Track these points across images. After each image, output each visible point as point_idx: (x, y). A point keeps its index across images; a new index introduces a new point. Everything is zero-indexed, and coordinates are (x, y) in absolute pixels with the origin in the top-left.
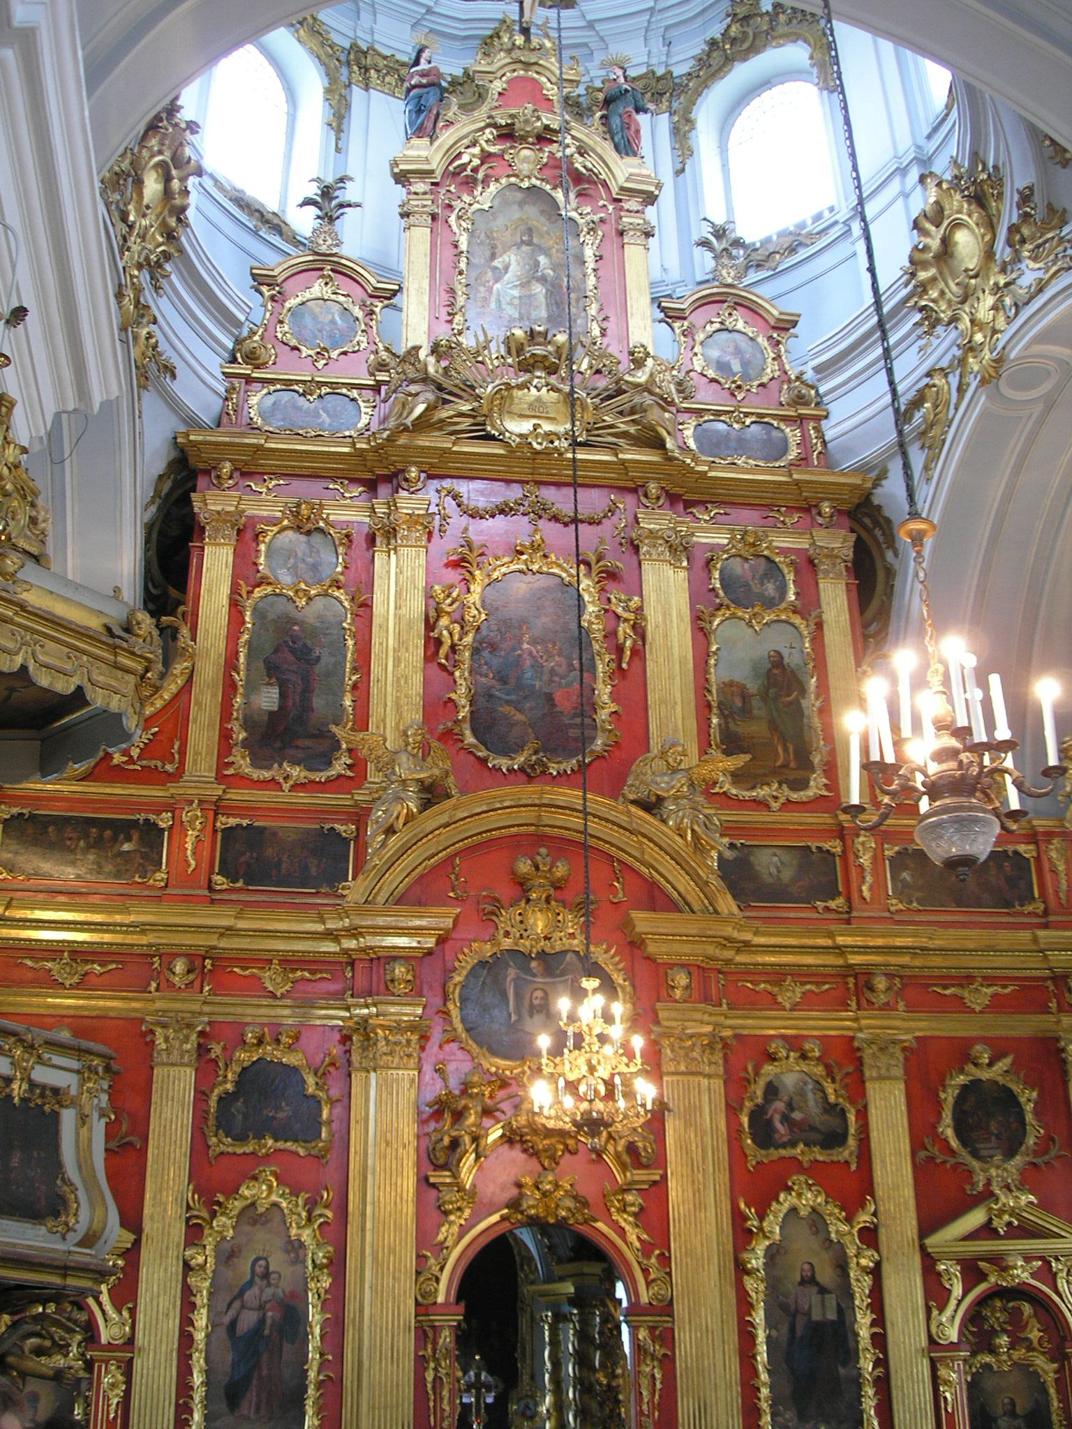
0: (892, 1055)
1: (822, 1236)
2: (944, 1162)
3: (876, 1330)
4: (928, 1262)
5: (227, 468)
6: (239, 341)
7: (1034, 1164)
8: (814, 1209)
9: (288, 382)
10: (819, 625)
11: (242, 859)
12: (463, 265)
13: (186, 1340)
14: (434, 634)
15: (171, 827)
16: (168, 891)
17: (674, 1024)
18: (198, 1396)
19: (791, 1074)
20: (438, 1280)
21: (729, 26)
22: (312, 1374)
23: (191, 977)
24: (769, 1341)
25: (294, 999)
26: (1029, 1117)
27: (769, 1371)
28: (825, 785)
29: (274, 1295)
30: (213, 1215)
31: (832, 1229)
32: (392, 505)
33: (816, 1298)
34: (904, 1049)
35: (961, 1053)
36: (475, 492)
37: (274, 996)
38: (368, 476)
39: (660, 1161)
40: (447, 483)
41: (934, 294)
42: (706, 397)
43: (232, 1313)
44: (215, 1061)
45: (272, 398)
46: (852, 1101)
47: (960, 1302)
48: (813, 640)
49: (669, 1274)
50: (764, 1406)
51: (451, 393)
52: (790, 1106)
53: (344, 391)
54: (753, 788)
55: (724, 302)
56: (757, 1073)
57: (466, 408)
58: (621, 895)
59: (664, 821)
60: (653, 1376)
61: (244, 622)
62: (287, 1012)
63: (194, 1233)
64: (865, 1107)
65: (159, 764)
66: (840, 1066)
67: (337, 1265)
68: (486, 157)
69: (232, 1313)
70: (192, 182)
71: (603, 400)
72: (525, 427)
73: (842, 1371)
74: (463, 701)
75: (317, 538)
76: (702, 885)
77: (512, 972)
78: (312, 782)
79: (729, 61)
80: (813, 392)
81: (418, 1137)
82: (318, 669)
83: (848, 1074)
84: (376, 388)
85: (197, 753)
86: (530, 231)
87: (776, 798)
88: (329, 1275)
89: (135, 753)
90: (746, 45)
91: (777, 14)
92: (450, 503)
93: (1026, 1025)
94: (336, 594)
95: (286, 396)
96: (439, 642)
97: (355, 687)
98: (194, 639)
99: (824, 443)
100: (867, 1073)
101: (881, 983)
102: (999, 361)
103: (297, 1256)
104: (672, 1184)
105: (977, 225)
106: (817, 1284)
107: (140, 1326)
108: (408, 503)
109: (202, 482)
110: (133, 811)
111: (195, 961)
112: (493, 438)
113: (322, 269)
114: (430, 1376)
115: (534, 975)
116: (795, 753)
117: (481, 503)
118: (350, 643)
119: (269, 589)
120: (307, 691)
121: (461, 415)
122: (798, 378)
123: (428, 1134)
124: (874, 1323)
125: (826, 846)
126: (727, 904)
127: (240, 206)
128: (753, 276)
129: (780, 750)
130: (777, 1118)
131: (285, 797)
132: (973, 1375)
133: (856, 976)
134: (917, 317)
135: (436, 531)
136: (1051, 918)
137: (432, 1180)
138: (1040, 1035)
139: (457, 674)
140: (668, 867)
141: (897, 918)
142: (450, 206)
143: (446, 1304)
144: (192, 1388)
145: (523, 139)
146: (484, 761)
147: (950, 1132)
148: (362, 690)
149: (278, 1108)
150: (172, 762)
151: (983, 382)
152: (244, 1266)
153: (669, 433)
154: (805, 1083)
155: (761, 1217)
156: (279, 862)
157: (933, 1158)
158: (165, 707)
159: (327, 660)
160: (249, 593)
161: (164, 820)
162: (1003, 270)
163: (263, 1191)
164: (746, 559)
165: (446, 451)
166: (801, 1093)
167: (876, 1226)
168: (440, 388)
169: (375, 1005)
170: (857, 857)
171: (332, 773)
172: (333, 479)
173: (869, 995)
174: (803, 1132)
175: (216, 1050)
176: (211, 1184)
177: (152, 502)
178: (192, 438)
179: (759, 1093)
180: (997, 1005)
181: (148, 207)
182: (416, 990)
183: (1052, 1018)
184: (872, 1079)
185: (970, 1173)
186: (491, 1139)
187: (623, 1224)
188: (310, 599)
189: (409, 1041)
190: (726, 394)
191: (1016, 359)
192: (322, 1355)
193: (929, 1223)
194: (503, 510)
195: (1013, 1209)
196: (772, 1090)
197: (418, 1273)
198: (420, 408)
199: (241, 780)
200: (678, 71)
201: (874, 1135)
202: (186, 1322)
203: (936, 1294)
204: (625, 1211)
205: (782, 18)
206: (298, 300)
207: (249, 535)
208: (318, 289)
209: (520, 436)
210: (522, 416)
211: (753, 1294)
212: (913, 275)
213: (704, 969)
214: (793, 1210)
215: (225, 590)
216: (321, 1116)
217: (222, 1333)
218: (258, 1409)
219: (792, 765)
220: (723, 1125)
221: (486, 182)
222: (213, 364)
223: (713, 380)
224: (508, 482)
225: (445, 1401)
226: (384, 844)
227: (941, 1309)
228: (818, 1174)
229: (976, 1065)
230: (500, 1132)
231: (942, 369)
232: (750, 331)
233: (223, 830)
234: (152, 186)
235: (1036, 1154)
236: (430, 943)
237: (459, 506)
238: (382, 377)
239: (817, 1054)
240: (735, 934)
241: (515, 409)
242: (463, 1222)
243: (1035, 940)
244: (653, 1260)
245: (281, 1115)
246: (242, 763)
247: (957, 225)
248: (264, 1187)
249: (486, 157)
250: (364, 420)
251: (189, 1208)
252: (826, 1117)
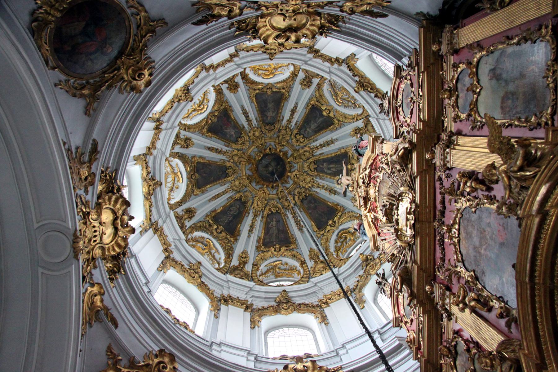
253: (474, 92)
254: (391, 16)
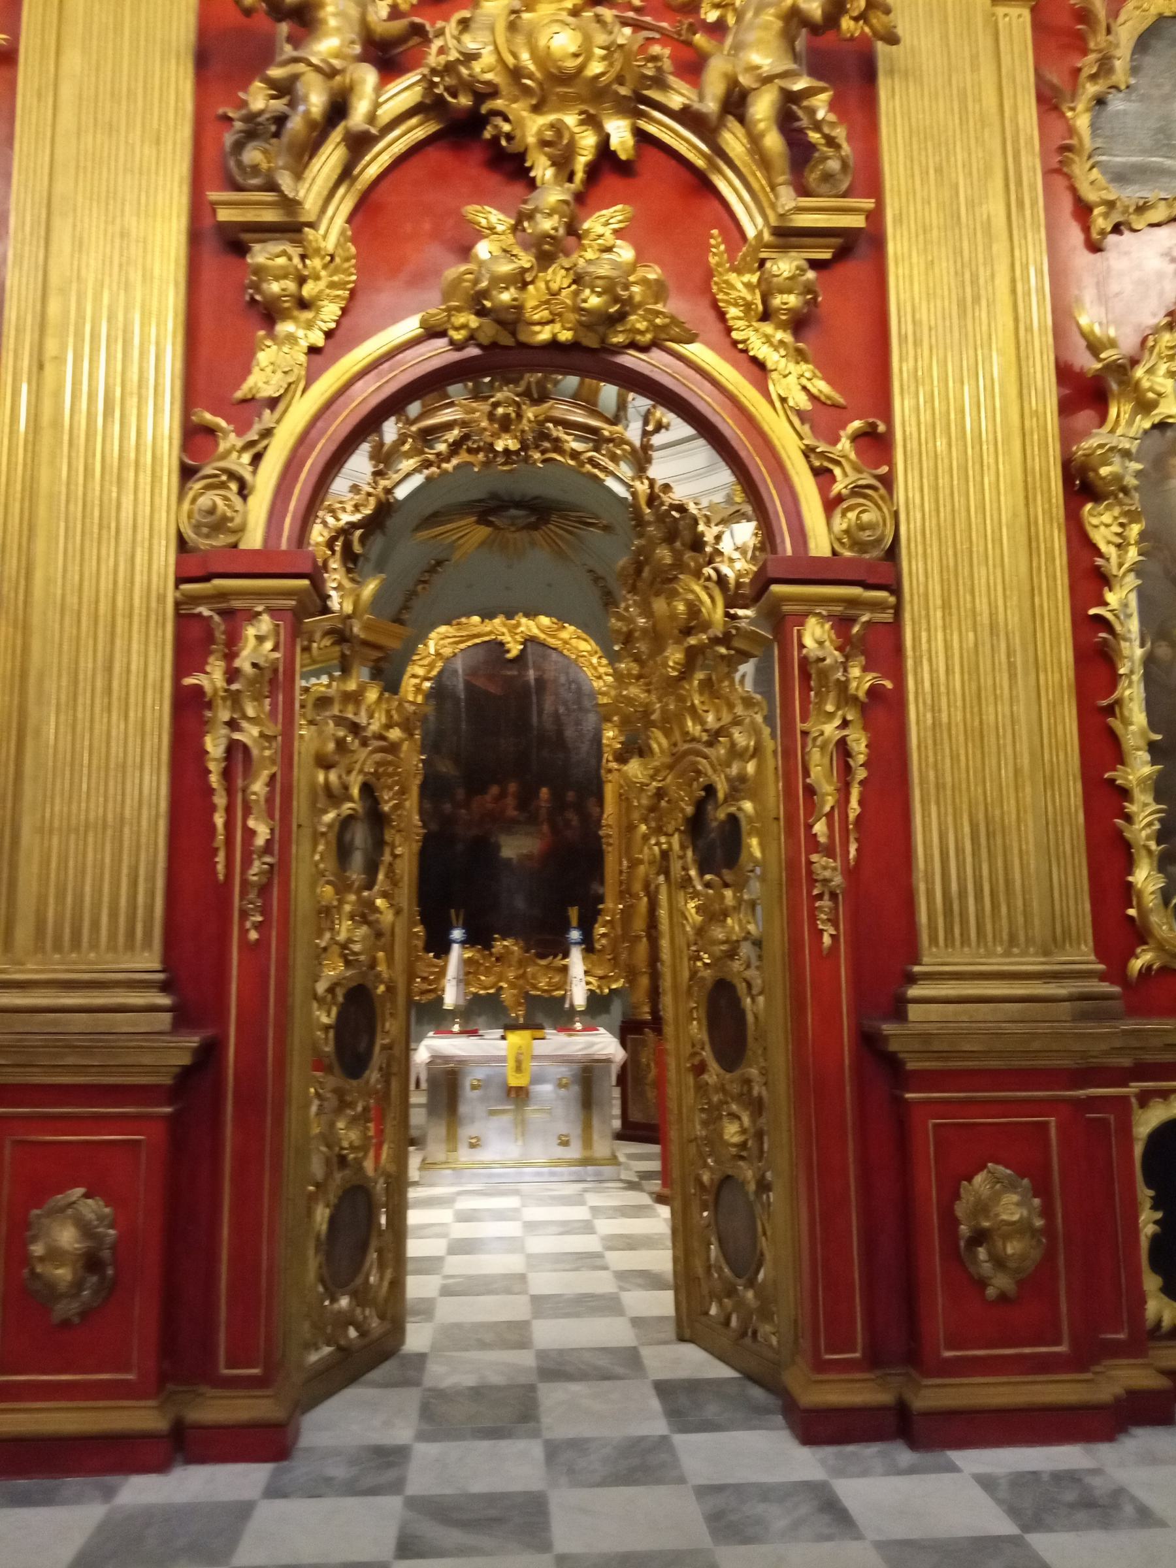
20: (244, 491)
60: (842, 744)
187: (760, 350)
204: (765, 316)
242: (318, 339)
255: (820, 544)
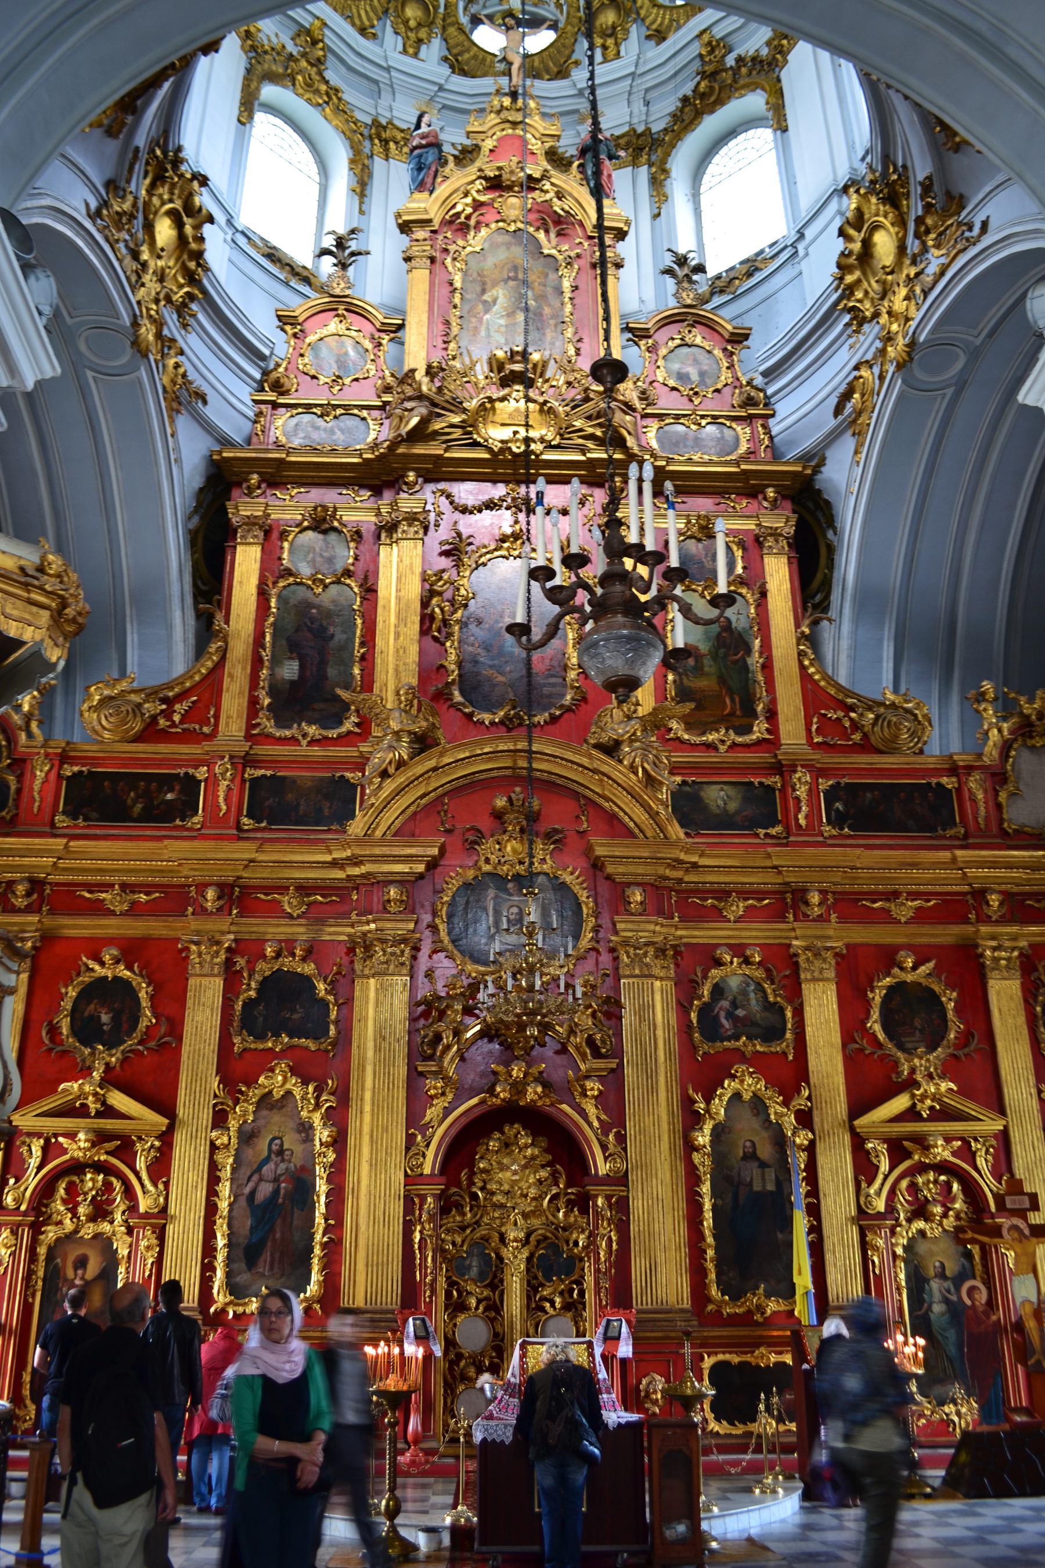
0: (825, 960)
1: (762, 1117)
2: (873, 1053)
3: (810, 1200)
4: (858, 1142)
5: (255, 478)
6: (265, 373)
7: (954, 1056)
8: (755, 1094)
9: (308, 407)
10: (764, 594)
11: (267, 803)
12: (457, 300)
13: (211, 1209)
14: (428, 611)
15: (206, 780)
16: (203, 831)
17: (630, 934)
18: (221, 1257)
19: (735, 978)
20: (424, 1156)
21: (699, 83)
22: (318, 1237)
23: (222, 902)
24: (714, 1209)
25: (307, 918)
26: (950, 1014)
27: (714, 1236)
28: (767, 730)
29: (287, 1169)
30: (237, 1101)
31: (772, 1111)
32: (394, 505)
33: (756, 1172)
34: (836, 955)
35: (887, 958)
36: (467, 492)
37: (290, 917)
38: (377, 482)
39: (617, 1053)
40: (442, 485)
41: (859, 295)
42: (667, 402)
43: (251, 1185)
44: (239, 972)
45: (295, 420)
46: (790, 1001)
47: (886, 1177)
48: (758, 606)
49: (625, 1149)
50: (710, 1266)
51: (443, 408)
52: (734, 1005)
53: (356, 411)
54: (703, 734)
55: (683, 321)
56: (705, 977)
57: (456, 419)
58: (585, 825)
59: (620, 761)
61: (270, 607)
62: (302, 930)
63: (220, 1119)
64: (801, 1005)
65: (197, 727)
66: (779, 971)
67: (339, 1142)
68: (477, 205)
69: (251, 1185)
70: (207, 229)
71: (573, 408)
72: (506, 433)
73: (780, 1236)
74: (453, 667)
75: (333, 537)
76: (653, 815)
77: (491, 893)
78: (326, 738)
79: (698, 115)
80: (762, 395)
81: (410, 1033)
82: (333, 644)
83: (786, 976)
84: (382, 408)
85: (228, 717)
86: (515, 268)
87: (723, 742)
88: (334, 1151)
89: (177, 718)
90: (712, 99)
91: (739, 68)
92: (443, 501)
93: (947, 934)
94: (348, 581)
95: (307, 418)
96: (432, 617)
97: (363, 658)
98: (227, 622)
99: (771, 438)
100: (803, 976)
101: (815, 898)
102: (912, 345)
103: (307, 1136)
104: (628, 1071)
105: (892, 224)
106: (758, 1159)
107: (173, 1197)
108: (407, 503)
109: (235, 493)
110: (174, 767)
111: (225, 890)
112: (479, 444)
113: (336, 309)
114: (417, 1237)
115: (511, 895)
116: (741, 703)
117: (471, 501)
118: (359, 621)
119: (291, 579)
120: (323, 663)
121: (452, 426)
122: (749, 383)
123: (418, 1030)
124: (808, 1195)
125: (768, 781)
126: (676, 831)
127: (273, 261)
128: (717, 300)
129: (728, 701)
130: (722, 1014)
131: (303, 749)
132: (909, 1239)
133: (793, 892)
134: (847, 318)
135: (432, 526)
136: (971, 841)
137: (420, 1069)
138: (961, 942)
139: (448, 644)
140: (625, 802)
141: (830, 842)
142: (446, 251)
143: (432, 1174)
144: (216, 1250)
145: (510, 188)
146: (469, 716)
147: (877, 1028)
148: (368, 660)
149: (293, 1011)
150: (208, 724)
151: (899, 367)
152: (262, 1146)
153: (630, 433)
154: (748, 985)
155: (708, 1100)
156: (298, 805)
157: (862, 1050)
158: (202, 681)
159: (339, 637)
160: (275, 583)
161: (202, 773)
162: (914, 263)
163: (277, 1080)
164: (699, 540)
165: (439, 457)
166: (744, 993)
167: (811, 1109)
168: (435, 405)
169: (374, 921)
170: (794, 790)
171: (343, 729)
172: (345, 486)
173: (803, 908)
174: (745, 1026)
175: (241, 962)
176: (235, 1072)
177: (196, 510)
178: (225, 455)
179: (706, 993)
180: (921, 917)
181: (162, 250)
182: (409, 907)
183: (971, 929)
184: (807, 980)
185: (896, 1063)
186: (469, 1034)
188: (326, 586)
189: (402, 952)
190: (685, 399)
191: (925, 341)
192: (326, 1220)
193: (858, 1107)
194: (490, 505)
195: (934, 1095)
196: (718, 991)
197: (408, 1149)
198: (415, 421)
199: (269, 739)
200: (656, 128)
201: (809, 1030)
202: (212, 1192)
203: (864, 1168)
205: (744, 70)
206: (317, 337)
207: (275, 535)
208: (334, 325)
209: (502, 442)
210: (503, 425)
211: (701, 1168)
212: (841, 279)
213: (657, 887)
214: (737, 1096)
215: (254, 581)
216: (328, 1016)
217: (243, 1202)
218: (272, 1268)
219: (738, 713)
220: (673, 1021)
221: (477, 226)
222: (244, 393)
223: (673, 389)
224: (495, 482)
225: (429, 1259)
226: (380, 787)
227: (870, 1184)
228: (760, 1064)
229: (902, 969)
230: (478, 1028)
231: (867, 362)
232: (706, 345)
233: (251, 780)
234: (164, 231)
235: (957, 1047)
236: (421, 868)
237: (451, 503)
238: (387, 398)
239: (758, 959)
240: (682, 856)
241: (498, 418)
243: (954, 859)
244: (611, 1137)
245: (295, 1016)
246: (267, 724)
247: (876, 227)
248: (280, 1078)
249: (477, 205)
250: (373, 435)
251: (216, 1096)
252: (767, 1014)
253: (705, 588)
254: (832, 423)
255: (603, 1167)
